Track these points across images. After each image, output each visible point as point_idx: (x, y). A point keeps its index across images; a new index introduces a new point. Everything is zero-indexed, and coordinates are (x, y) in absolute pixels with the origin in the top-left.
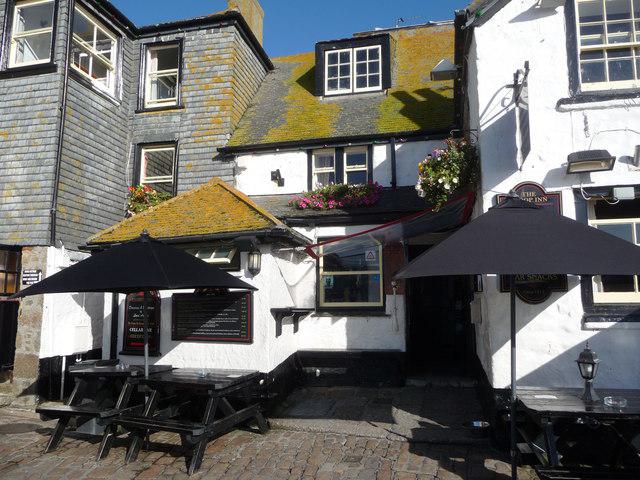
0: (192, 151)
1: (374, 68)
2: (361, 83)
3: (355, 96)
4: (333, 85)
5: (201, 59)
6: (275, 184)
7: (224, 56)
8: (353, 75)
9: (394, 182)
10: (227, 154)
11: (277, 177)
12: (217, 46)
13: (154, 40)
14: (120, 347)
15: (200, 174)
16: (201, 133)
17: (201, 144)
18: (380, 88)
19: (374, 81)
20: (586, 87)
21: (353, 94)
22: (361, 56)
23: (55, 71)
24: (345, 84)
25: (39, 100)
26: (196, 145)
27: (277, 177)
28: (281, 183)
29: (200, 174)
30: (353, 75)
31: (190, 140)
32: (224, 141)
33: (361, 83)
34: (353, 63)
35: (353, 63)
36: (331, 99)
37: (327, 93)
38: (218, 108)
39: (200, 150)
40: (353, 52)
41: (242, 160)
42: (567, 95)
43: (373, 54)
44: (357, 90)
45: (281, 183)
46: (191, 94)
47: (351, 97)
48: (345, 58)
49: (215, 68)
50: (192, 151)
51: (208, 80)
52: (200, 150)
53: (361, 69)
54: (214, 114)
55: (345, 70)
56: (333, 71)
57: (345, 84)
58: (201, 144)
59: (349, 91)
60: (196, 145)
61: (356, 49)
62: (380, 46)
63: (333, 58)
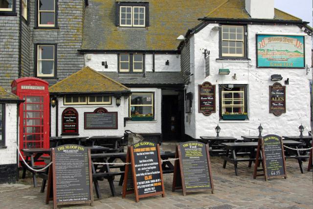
0: (63, 49)
1: (142, 16)
2: (136, 22)
3: (134, 28)
4: (123, 23)
5: (67, 6)
6: (104, 67)
7: (78, 7)
8: (133, 19)
9: (154, 70)
10: (82, 52)
11: (105, 64)
14: (60, 132)
15: (68, 60)
17: (68, 47)
18: (144, 26)
20: (224, 55)
21: (132, 27)
22: (136, 10)
23: (16, 15)
24: (129, 22)
25: (8, 28)
26: (65, 47)
27: (105, 64)
28: (106, 67)
29: (68, 60)
30: (133, 19)
31: (62, 44)
32: (78, 46)
33: (136, 22)
34: (133, 13)
35: (133, 13)
36: (122, 28)
37: (121, 25)
38: (76, 31)
39: (68, 49)
40: (133, 8)
41: (88, 56)
42: (218, 57)
44: (134, 26)
45: (106, 67)
46: (62, 22)
47: (132, 28)
48: (129, 10)
49: (74, 12)
50: (63, 49)
51: (70, 17)
52: (68, 49)
53: (136, 16)
54: (74, 33)
55: (129, 16)
56: (123, 16)
58: (68, 47)
59: (131, 26)
60: (65, 47)
62: (144, 7)
63: (123, 10)
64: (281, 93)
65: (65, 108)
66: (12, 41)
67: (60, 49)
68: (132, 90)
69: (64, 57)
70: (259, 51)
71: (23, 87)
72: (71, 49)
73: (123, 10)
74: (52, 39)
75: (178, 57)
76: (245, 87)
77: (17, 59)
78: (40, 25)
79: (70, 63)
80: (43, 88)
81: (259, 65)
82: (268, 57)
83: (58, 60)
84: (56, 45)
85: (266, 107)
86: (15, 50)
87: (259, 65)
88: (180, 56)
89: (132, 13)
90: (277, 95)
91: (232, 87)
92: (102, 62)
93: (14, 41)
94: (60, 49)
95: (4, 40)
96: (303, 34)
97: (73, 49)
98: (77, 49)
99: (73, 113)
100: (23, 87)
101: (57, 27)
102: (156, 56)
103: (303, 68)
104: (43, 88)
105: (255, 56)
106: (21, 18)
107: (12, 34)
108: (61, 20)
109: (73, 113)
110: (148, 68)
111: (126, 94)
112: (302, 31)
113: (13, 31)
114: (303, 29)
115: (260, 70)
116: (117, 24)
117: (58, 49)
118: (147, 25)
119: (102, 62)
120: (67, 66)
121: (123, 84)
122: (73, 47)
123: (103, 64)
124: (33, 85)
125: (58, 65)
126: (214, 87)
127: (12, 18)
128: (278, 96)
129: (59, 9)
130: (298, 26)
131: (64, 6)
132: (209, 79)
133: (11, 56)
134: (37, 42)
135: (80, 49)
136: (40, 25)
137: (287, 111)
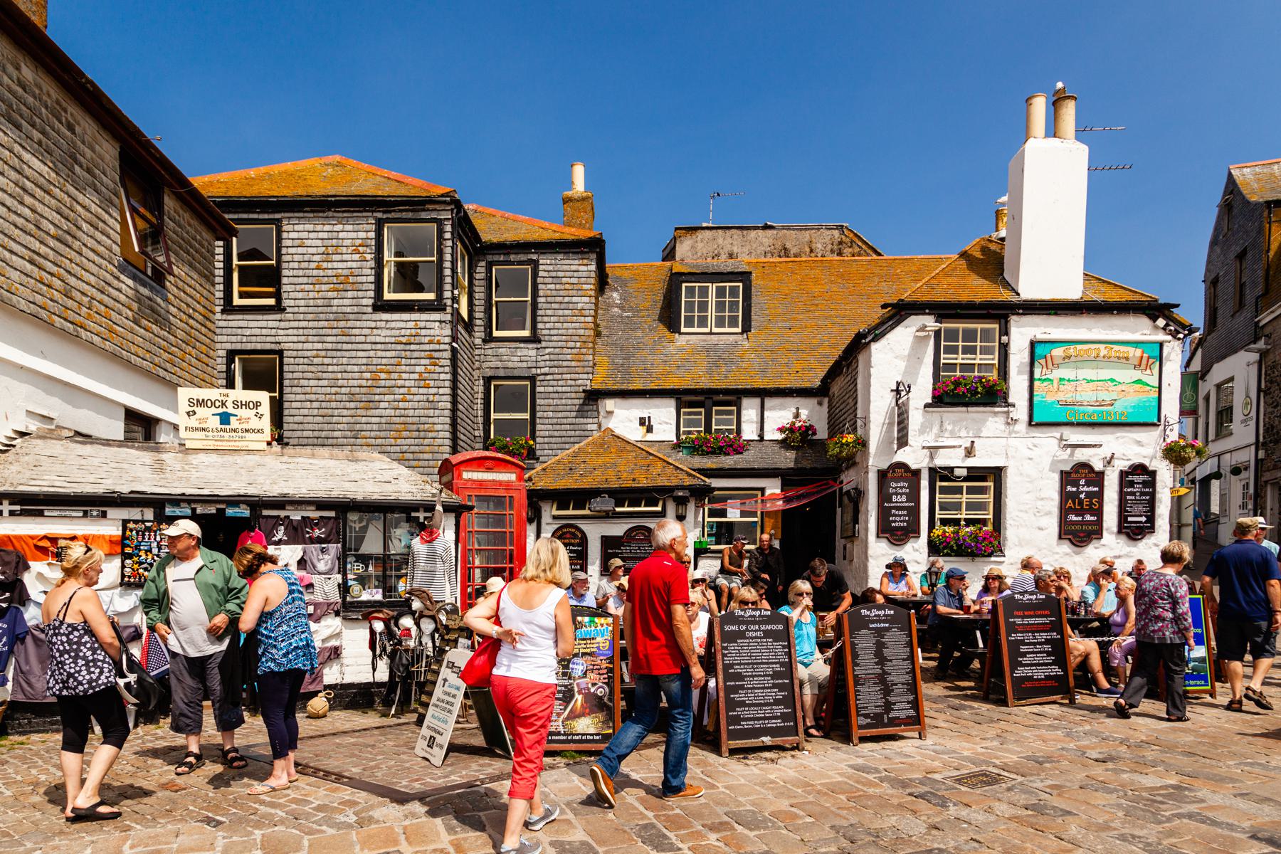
0: (551, 389)
1: (734, 305)
2: (720, 322)
4: (690, 323)
5: (558, 287)
6: (644, 429)
8: (712, 313)
10: (593, 397)
11: (646, 423)
12: (576, 274)
13: (502, 258)
15: (560, 415)
16: (561, 370)
17: (560, 383)
18: (739, 330)
19: (733, 323)
22: (721, 293)
23: (445, 310)
24: (703, 322)
25: (426, 340)
26: (555, 383)
27: (646, 423)
29: (560, 415)
30: (712, 313)
33: (720, 322)
34: (712, 299)
35: (712, 299)
36: (688, 337)
37: (683, 330)
39: (560, 389)
40: (712, 288)
41: (610, 404)
43: (734, 292)
44: (715, 330)
45: (650, 429)
46: (548, 326)
48: (704, 292)
50: (551, 389)
53: (720, 306)
55: (703, 306)
56: (690, 306)
57: (703, 322)
58: (560, 383)
59: (707, 330)
60: (555, 383)
61: (715, 285)
62: (741, 284)
63: (691, 291)
64: (1091, 489)
65: (556, 526)
66: (438, 369)
67: (542, 389)
68: (715, 483)
69: (551, 408)
70: (1037, 384)
71: (466, 475)
72: (568, 389)
73: (691, 291)
74: (525, 365)
75: (820, 404)
76: (996, 474)
77: (447, 413)
78: (496, 333)
79: (565, 421)
80: (513, 477)
81: (1036, 419)
82: (1061, 397)
83: (539, 415)
84: (532, 379)
85: (1052, 524)
86: (441, 391)
87: (1036, 419)
88: (826, 400)
89: (714, 299)
90: (1082, 492)
91: (964, 472)
92: (641, 419)
93: (441, 370)
94: (542, 389)
95: (418, 369)
96: (1161, 337)
97: (573, 389)
98: (581, 389)
99: (574, 536)
100: (466, 475)
101: (535, 339)
102: (769, 402)
103: (1153, 425)
104: (513, 477)
105: (1026, 395)
106: (456, 313)
107: (436, 355)
108: (546, 319)
109: (574, 536)
110: (749, 432)
111: (700, 493)
112: (1156, 327)
113: (437, 347)
114: (1161, 322)
115: (1037, 433)
116: (673, 326)
117: (538, 389)
118: (746, 329)
119: (641, 419)
120: (558, 427)
121: (694, 470)
122: (572, 383)
123: (642, 422)
124: (489, 469)
125: (538, 427)
126: (917, 473)
127: (436, 316)
128: (1082, 496)
129: (541, 293)
130: (1144, 313)
131: (552, 286)
132: (903, 456)
133: (432, 405)
134: (489, 373)
135: (588, 388)
136: (496, 333)
137: (1105, 533)
